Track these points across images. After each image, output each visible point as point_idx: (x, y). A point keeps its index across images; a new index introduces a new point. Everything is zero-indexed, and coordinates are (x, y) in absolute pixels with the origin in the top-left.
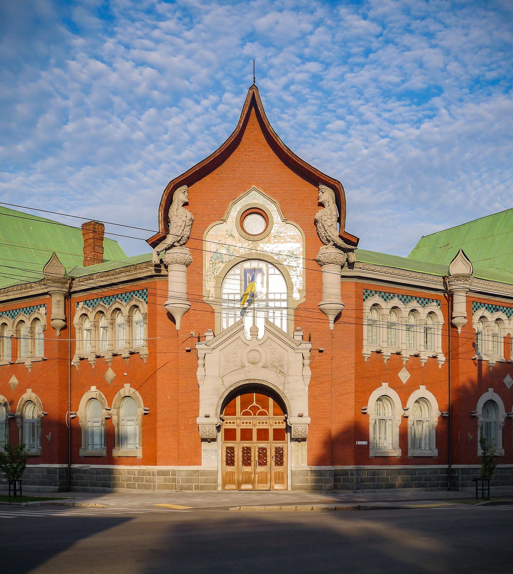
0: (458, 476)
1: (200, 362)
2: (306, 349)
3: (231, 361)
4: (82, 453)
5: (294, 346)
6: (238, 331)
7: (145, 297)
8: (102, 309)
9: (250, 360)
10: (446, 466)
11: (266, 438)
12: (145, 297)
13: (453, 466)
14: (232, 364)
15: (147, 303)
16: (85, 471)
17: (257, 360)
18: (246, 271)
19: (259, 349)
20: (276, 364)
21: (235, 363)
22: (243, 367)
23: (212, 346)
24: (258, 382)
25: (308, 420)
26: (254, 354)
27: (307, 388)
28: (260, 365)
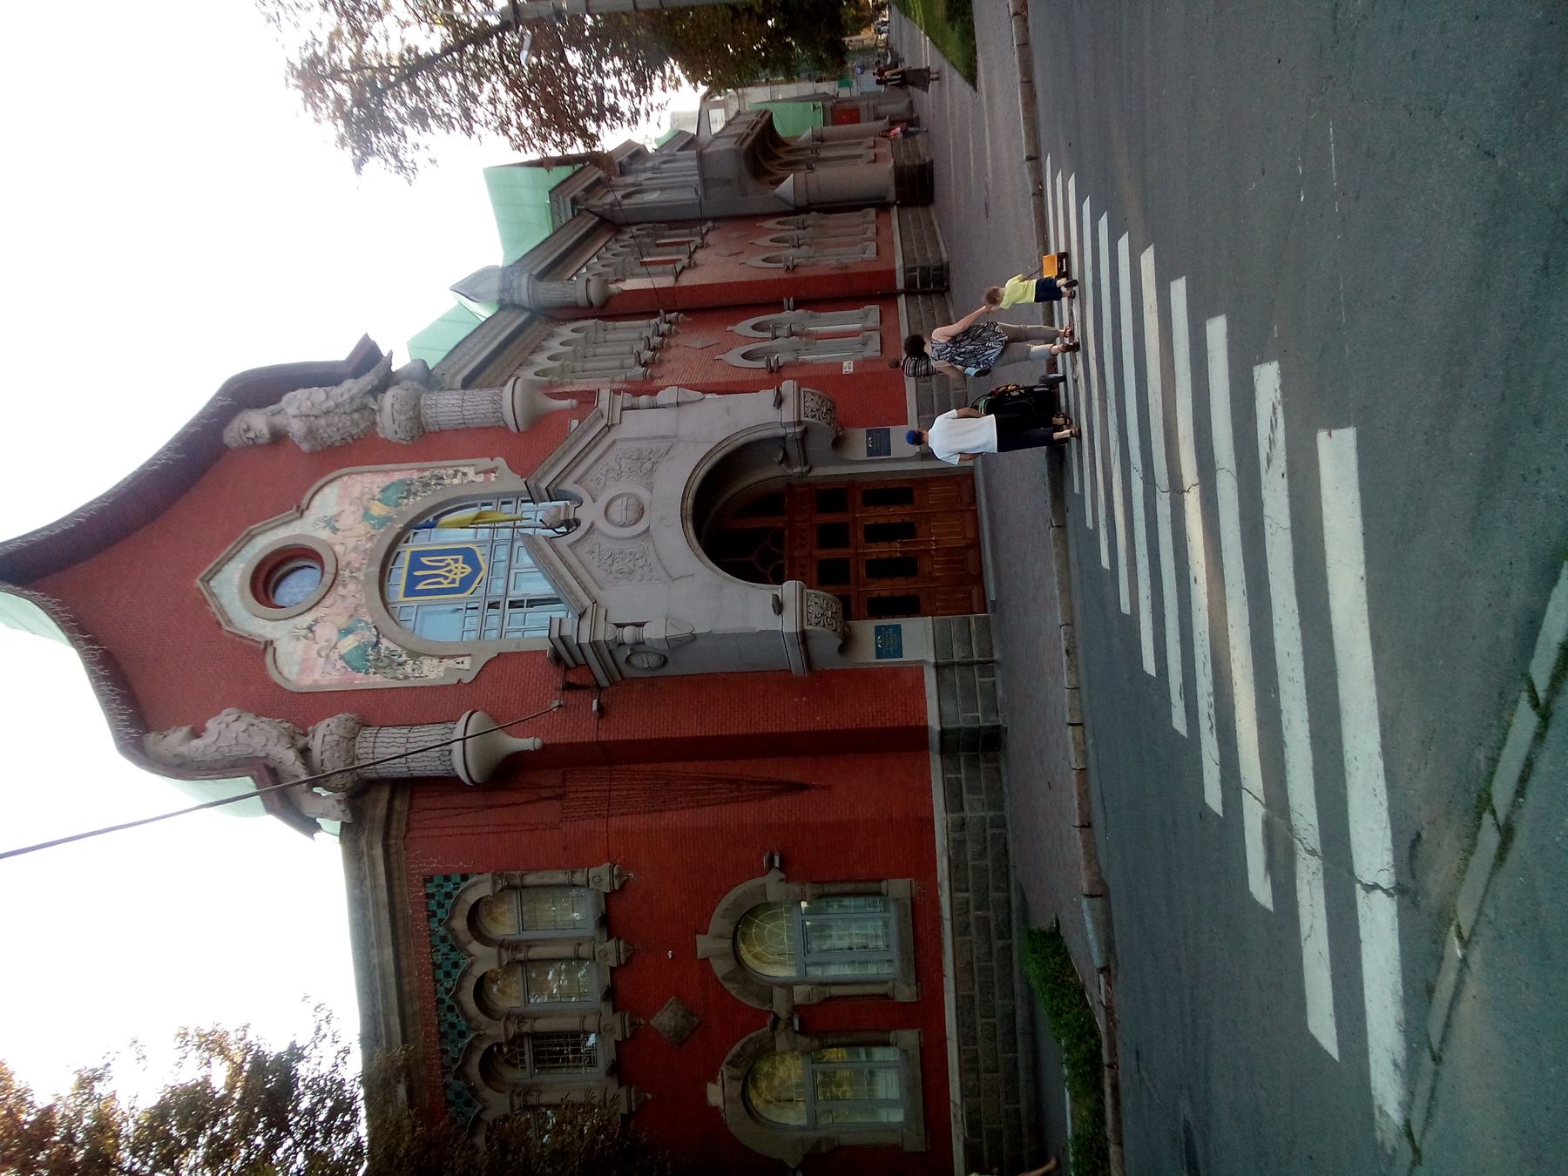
0: (922, 268)
1: (628, 634)
2: (612, 402)
4: (915, 1142)
5: (604, 422)
6: (554, 548)
7: (449, 887)
8: (476, 1059)
9: (632, 515)
10: (902, 301)
11: (843, 564)
12: (449, 887)
13: (900, 285)
14: (641, 562)
15: (465, 878)
16: (973, 1127)
17: (631, 501)
18: (410, 591)
19: (603, 500)
20: (648, 465)
22: (647, 530)
23: (588, 602)
24: (690, 502)
25: (788, 387)
26: (617, 511)
27: (709, 396)
28: (644, 494)
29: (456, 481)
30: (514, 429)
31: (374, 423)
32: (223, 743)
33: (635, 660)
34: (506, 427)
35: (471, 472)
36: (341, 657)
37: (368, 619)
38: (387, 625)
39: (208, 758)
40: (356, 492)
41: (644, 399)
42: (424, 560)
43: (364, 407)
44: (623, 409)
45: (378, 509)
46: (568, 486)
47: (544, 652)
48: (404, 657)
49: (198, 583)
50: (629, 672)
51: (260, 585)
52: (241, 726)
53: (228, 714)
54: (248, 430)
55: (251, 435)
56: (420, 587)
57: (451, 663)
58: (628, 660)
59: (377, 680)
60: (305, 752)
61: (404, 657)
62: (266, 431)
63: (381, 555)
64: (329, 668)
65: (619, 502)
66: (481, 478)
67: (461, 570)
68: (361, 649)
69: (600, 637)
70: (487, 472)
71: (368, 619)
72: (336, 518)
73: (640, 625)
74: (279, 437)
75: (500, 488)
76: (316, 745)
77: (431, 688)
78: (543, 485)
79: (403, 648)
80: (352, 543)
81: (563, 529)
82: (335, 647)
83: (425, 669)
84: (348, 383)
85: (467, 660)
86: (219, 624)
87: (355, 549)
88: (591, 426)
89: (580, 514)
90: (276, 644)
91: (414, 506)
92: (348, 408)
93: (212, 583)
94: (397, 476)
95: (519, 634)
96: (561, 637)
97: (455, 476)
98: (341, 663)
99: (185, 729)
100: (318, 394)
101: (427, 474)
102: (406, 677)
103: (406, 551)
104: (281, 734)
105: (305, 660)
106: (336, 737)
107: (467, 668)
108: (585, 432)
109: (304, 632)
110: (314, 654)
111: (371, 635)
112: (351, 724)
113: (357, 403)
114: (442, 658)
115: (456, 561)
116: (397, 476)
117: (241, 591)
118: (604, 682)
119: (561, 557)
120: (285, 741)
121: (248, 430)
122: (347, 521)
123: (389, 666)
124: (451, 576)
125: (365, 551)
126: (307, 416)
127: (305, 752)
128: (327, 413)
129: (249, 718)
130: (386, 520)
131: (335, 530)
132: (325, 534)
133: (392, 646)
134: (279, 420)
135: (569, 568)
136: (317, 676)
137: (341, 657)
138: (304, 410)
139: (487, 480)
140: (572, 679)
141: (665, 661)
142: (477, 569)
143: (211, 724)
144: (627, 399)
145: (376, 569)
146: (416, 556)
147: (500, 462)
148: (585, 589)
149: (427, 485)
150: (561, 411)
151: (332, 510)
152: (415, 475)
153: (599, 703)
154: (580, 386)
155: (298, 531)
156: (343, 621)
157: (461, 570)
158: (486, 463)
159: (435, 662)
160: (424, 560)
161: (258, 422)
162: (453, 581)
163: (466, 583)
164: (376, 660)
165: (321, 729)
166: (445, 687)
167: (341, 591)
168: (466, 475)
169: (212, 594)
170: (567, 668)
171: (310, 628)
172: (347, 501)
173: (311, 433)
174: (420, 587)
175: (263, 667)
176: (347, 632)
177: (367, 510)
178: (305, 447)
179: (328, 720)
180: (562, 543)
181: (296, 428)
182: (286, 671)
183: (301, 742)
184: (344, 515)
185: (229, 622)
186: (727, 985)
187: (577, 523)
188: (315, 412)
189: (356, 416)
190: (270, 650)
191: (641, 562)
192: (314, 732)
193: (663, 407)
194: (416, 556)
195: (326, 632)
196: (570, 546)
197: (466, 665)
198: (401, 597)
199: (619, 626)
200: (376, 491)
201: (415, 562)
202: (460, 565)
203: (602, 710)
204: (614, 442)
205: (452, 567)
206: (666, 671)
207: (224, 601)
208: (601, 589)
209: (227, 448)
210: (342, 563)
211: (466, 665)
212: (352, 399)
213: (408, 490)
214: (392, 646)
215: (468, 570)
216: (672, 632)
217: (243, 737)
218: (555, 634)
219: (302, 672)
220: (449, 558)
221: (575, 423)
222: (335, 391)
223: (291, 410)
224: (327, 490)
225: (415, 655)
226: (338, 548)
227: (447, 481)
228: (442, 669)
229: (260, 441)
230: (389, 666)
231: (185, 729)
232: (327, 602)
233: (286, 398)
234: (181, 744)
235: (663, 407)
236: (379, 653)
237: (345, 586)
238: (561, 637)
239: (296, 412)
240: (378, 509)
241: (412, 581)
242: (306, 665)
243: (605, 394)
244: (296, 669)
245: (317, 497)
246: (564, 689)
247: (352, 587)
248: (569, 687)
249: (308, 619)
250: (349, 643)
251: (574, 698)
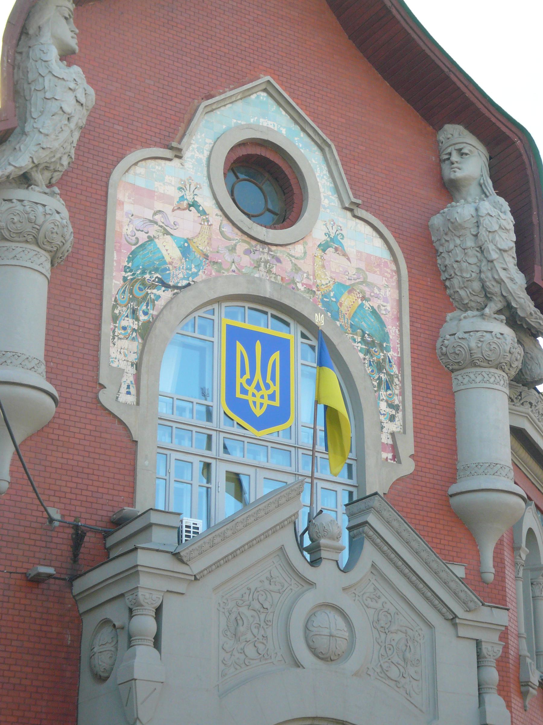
1: (145, 623)
2: (488, 627)
3: (249, 636)
6: (281, 525)
9: (322, 644)
14: (250, 651)
17: (343, 645)
18: (234, 334)
19: (346, 602)
20: (394, 673)
21: (261, 647)
22: (297, 664)
23: (196, 567)
26: (331, 622)
28: (352, 664)
29: (383, 406)
30: (453, 489)
31: (466, 308)
32: (48, 82)
33: (106, 634)
34: (454, 480)
35: (395, 427)
36: (151, 239)
37: (201, 276)
38: (189, 301)
39: (31, 64)
40: (372, 278)
41: (492, 675)
42: (276, 356)
43: (488, 296)
44: (478, 643)
45: (348, 302)
46: (369, 553)
47: (132, 504)
48: (143, 318)
49: (268, 78)
50: (90, 623)
51: (258, 151)
52: (69, 106)
53: (87, 94)
54: (461, 153)
55: (455, 157)
56: (240, 347)
57: (129, 378)
58: (107, 622)
59: (114, 282)
60: (25, 180)
61: (143, 318)
62: (459, 174)
63: (286, 301)
64: (138, 223)
65: (341, 622)
66: (386, 439)
67: (259, 402)
68: (160, 266)
69: (144, 581)
70: (394, 448)
71: (201, 276)
72: (340, 250)
73: (157, 642)
74: (449, 190)
75: (371, 462)
76: (34, 195)
77: (97, 349)
78: (372, 519)
79: (156, 318)
80: (306, 266)
81: (307, 542)
82: (168, 233)
83: (125, 343)
84: (520, 279)
85: (131, 399)
86: (209, 97)
87: (297, 269)
88: (455, 594)
89: (326, 567)
90: (176, 161)
91: (352, 350)
92: (487, 275)
93: (264, 94)
94: (392, 331)
95: (162, 473)
96: (149, 526)
97: (391, 406)
98: (143, 237)
99: (73, 43)
100: (508, 240)
101: (395, 370)
102: (115, 318)
103: (292, 335)
104: (54, 152)
105: (151, 194)
106: (40, 220)
107: (118, 397)
108: (445, 584)
109: (189, 197)
110: (159, 206)
111: (178, 277)
112: (58, 240)
113: (496, 289)
114: (138, 366)
115: (272, 397)
116: (392, 331)
117: (249, 127)
118: (80, 585)
119: (266, 535)
120: (43, 156)
121: (461, 153)
123: (134, 298)
124: (251, 389)
125: (293, 282)
126: (478, 225)
127: (25, 180)
128: (481, 249)
129: (80, 117)
130: (333, 310)
131: (324, 247)
132: (319, 234)
133: (160, 304)
134: (474, 190)
135: (250, 545)
136: (128, 207)
137: (151, 239)
138: (485, 221)
139: (384, 447)
140: (89, 539)
141: (101, 679)
142: (260, 423)
143: (76, 71)
144: (493, 649)
145: (268, 291)
146: (283, 346)
147: (408, 467)
148: (217, 565)
149: (380, 367)
150: (478, 554)
151: (349, 245)
152: (392, 354)
153: (50, 576)
154: (515, 589)
155: (325, 202)
156: (201, 244)
157: (259, 402)
158: (407, 447)
159: (133, 358)
160: (276, 356)
161: (472, 164)
162: (244, 391)
163: (240, 407)
164: (143, 282)
165: (56, 203)
166: (97, 368)
167: (242, 247)
168: (389, 424)
169: (246, 95)
170: (107, 535)
171: (194, 205)
172: (362, 266)
173: (454, 228)
174: (240, 347)
175: (146, 144)
176: (186, 250)
178: (437, 221)
179: (65, 213)
180: (286, 538)
181: (463, 211)
182: (140, 170)
183: (40, 177)
184: (343, 259)
185: (211, 110)
187: (315, 562)
188: (483, 232)
189: (476, 286)
190: (168, 153)
191: (250, 651)
192: (53, 194)
193: (481, 702)
194: (283, 346)
195: (187, 224)
196: (282, 549)
197: (124, 398)
198: (226, 321)
199: (158, 611)
200: (375, 303)
201: (273, 344)
202: (267, 402)
203: (37, 580)
204: (430, 626)
205: (266, 393)
206: (86, 681)
207: (239, 106)
208: (216, 589)
209: (438, 127)
210: (279, 252)
211: (124, 398)
212: (500, 282)
213: (373, 344)
214: (160, 304)
215: (258, 412)
216: (141, 691)
217: (53, 106)
218: (154, 518)
219: (136, 190)
220: (276, 388)
221: (460, 571)
222: (511, 261)
223: (486, 206)
224: (379, 242)
225: (145, 332)
226: (298, 249)
227: (383, 393)
228: (122, 365)
229: (445, 167)
230: (134, 298)
231: (73, 43)
232: (228, 228)
233: (501, 200)
234: (53, 36)
235: (481, 702)
236: (152, 286)
237: (247, 252)
238: (149, 526)
239: (483, 211)
241: (248, 338)
242: (144, 195)
243: (500, 617)
244: (141, 182)
245: (368, 229)
246: (76, 527)
247: (246, 260)
248: (78, 536)
249: (207, 202)
250: (169, 250)
251: (63, 541)
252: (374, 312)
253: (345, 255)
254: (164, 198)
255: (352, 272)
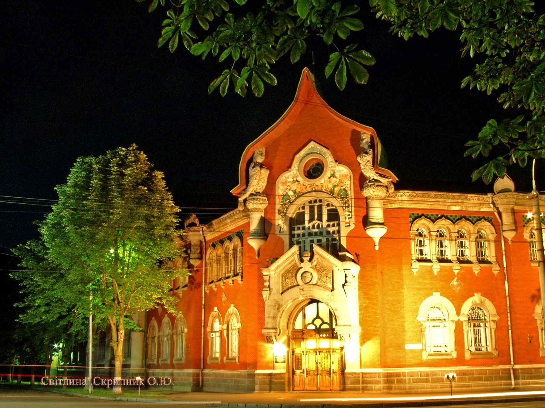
1: (266, 284)
45: (337, 189)
87: (323, 186)
98: (285, 193)
109: (295, 179)
110: (288, 184)
122: (333, 180)
131: (330, 178)
151: (337, 174)
171: (297, 181)
177: (337, 186)
184: (335, 179)
186: (227, 314)
195: (295, 187)
240: (337, 189)
250: (291, 193)
252: (344, 189)
253: (336, 177)
254: (290, 182)
255: (338, 180)
